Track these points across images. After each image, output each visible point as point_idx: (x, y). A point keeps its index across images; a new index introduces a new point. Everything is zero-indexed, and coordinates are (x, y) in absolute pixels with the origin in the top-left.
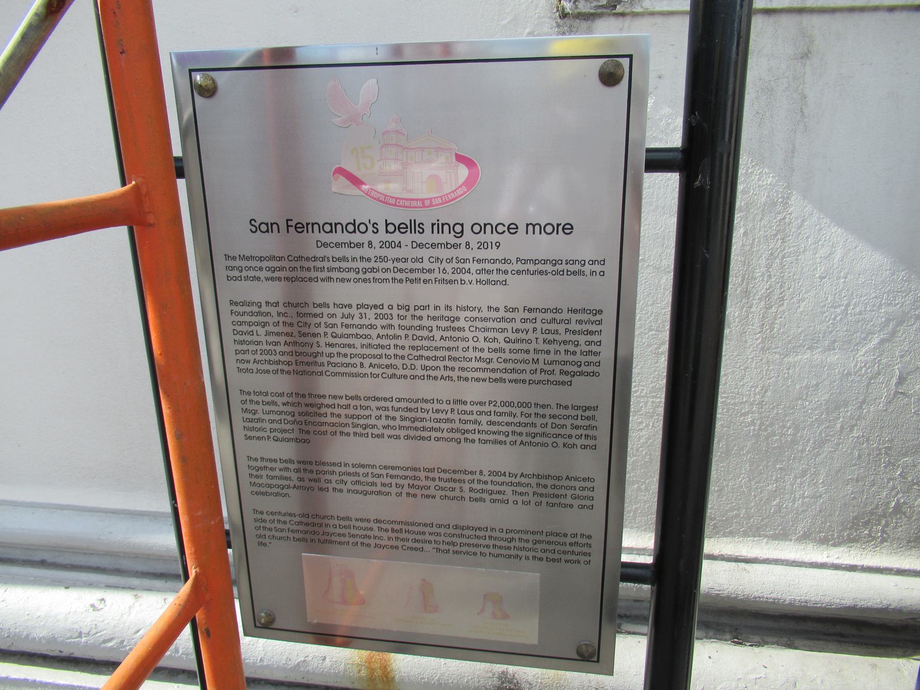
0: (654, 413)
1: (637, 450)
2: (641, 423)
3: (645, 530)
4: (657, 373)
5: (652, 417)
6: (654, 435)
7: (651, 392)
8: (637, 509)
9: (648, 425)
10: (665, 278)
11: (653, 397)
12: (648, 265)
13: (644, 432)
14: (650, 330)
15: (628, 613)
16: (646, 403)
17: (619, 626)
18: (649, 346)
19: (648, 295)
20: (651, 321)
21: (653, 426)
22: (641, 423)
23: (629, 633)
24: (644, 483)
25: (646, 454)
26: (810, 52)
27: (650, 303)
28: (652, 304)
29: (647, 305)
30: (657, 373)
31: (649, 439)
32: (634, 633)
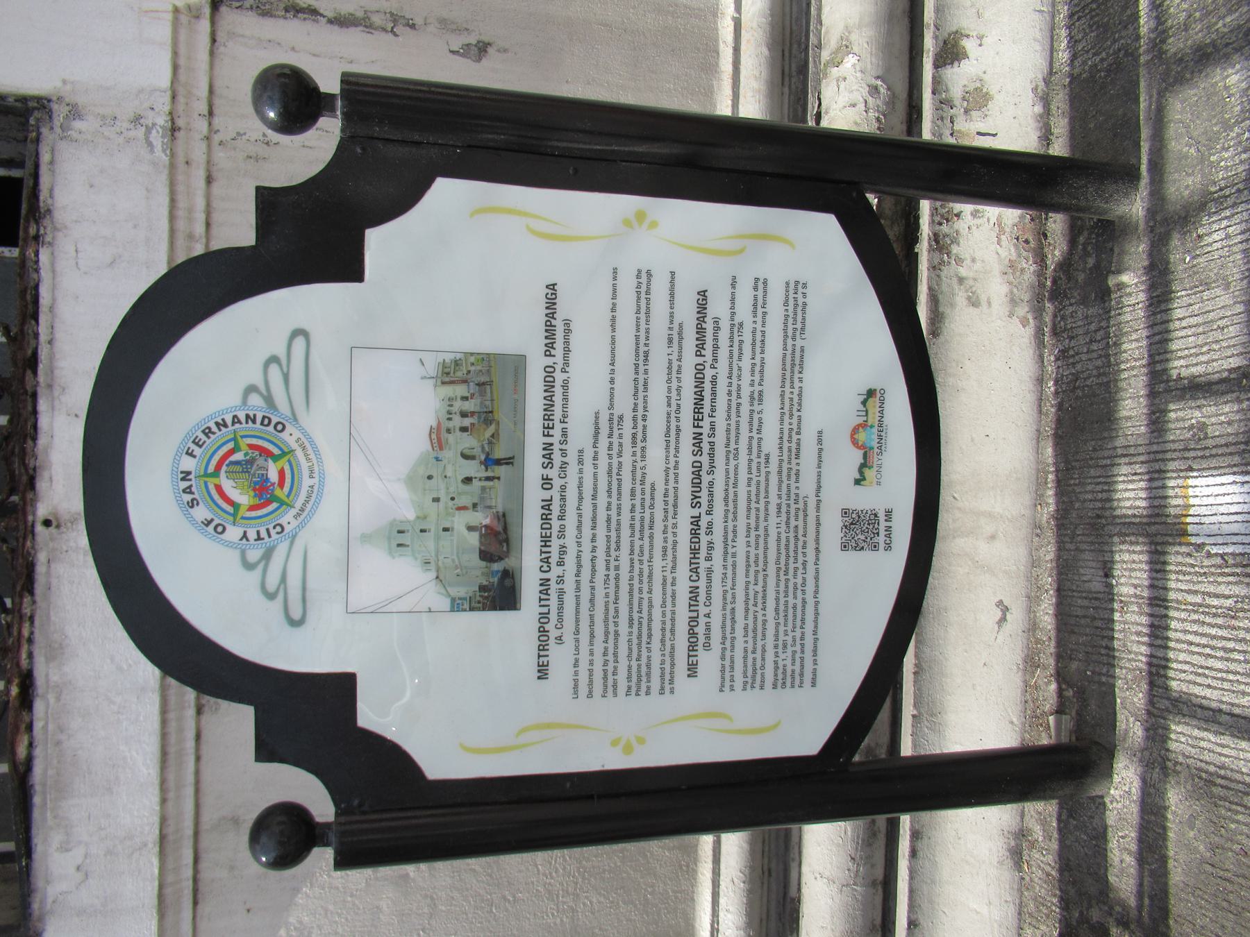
0: (574, 894)
1: (612, 902)
2: (584, 904)
3: (695, 879)
4: (534, 898)
5: (578, 895)
6: (596, 890)
7: (553, 900)
8: (673, 891)
9: (587, 897)
10: (440, 907)
11: (558, 897)
12: (429, 924)
13: (594, 900)
14: (491, 911)
15: (782, 885)
16: (564, 903)
17: (793, 900)
18: (507, 910)
19: (457, 920)
20: (483, 913)
21: (587, 892)
22: (584, 904)
23: (799, 890)
24: (646, 890)
25: (615, 893)
26: (233, 817)
27: (465, 916)
28: (466, 914)
29: (467, 919)
30: (534, 898)
31: (600, 894)
32: (799, 884)
